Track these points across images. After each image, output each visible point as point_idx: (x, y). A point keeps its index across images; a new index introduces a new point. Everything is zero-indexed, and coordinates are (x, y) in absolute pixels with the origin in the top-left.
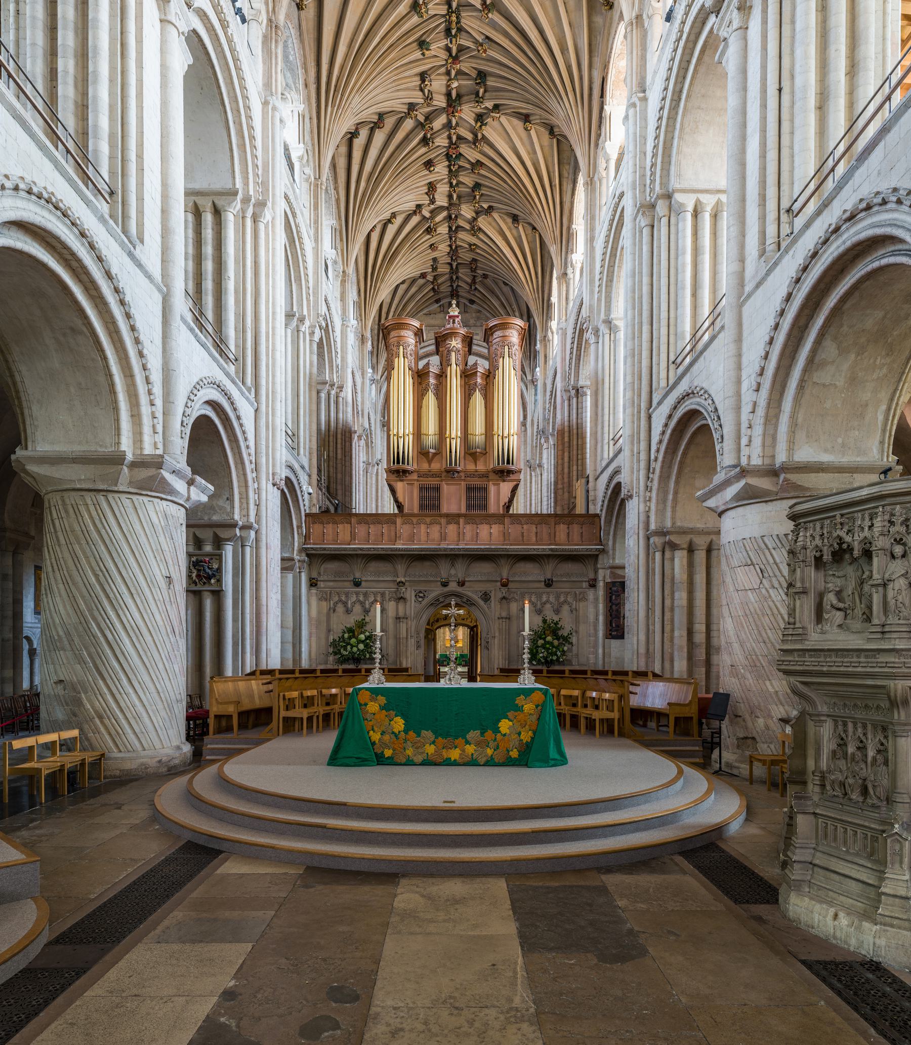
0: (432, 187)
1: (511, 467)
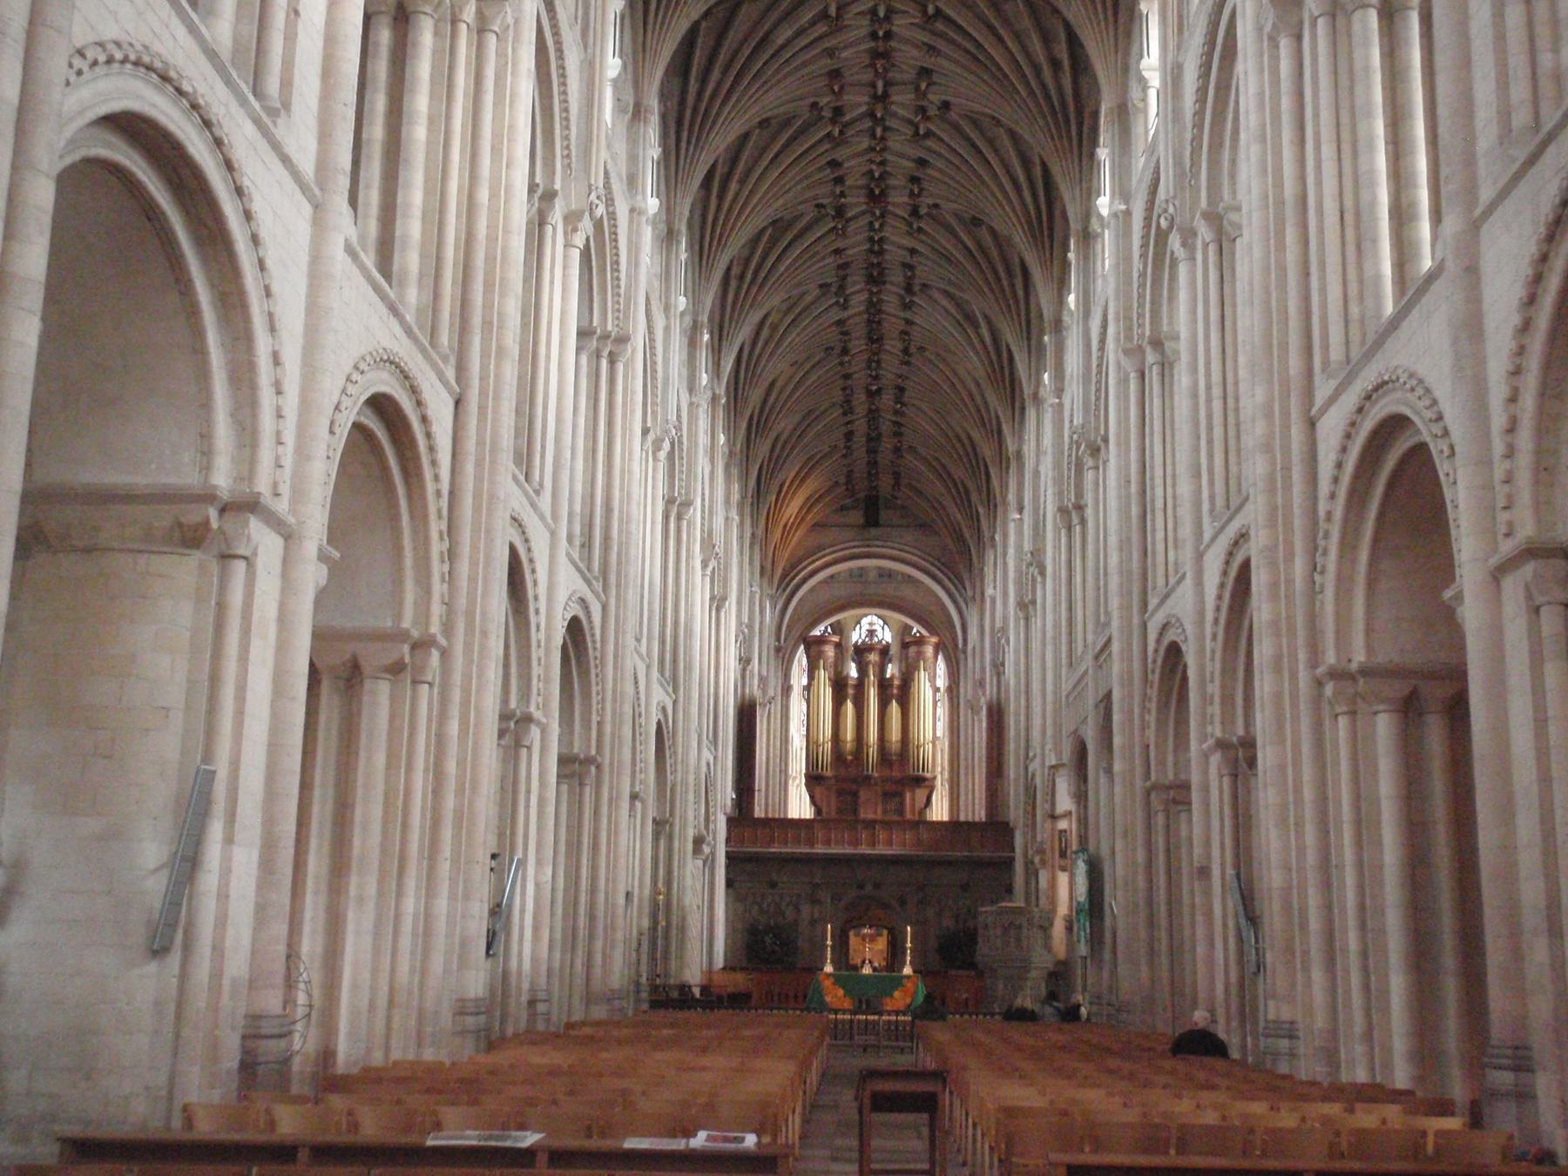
0: (849, 436)
1: (928, 775)
